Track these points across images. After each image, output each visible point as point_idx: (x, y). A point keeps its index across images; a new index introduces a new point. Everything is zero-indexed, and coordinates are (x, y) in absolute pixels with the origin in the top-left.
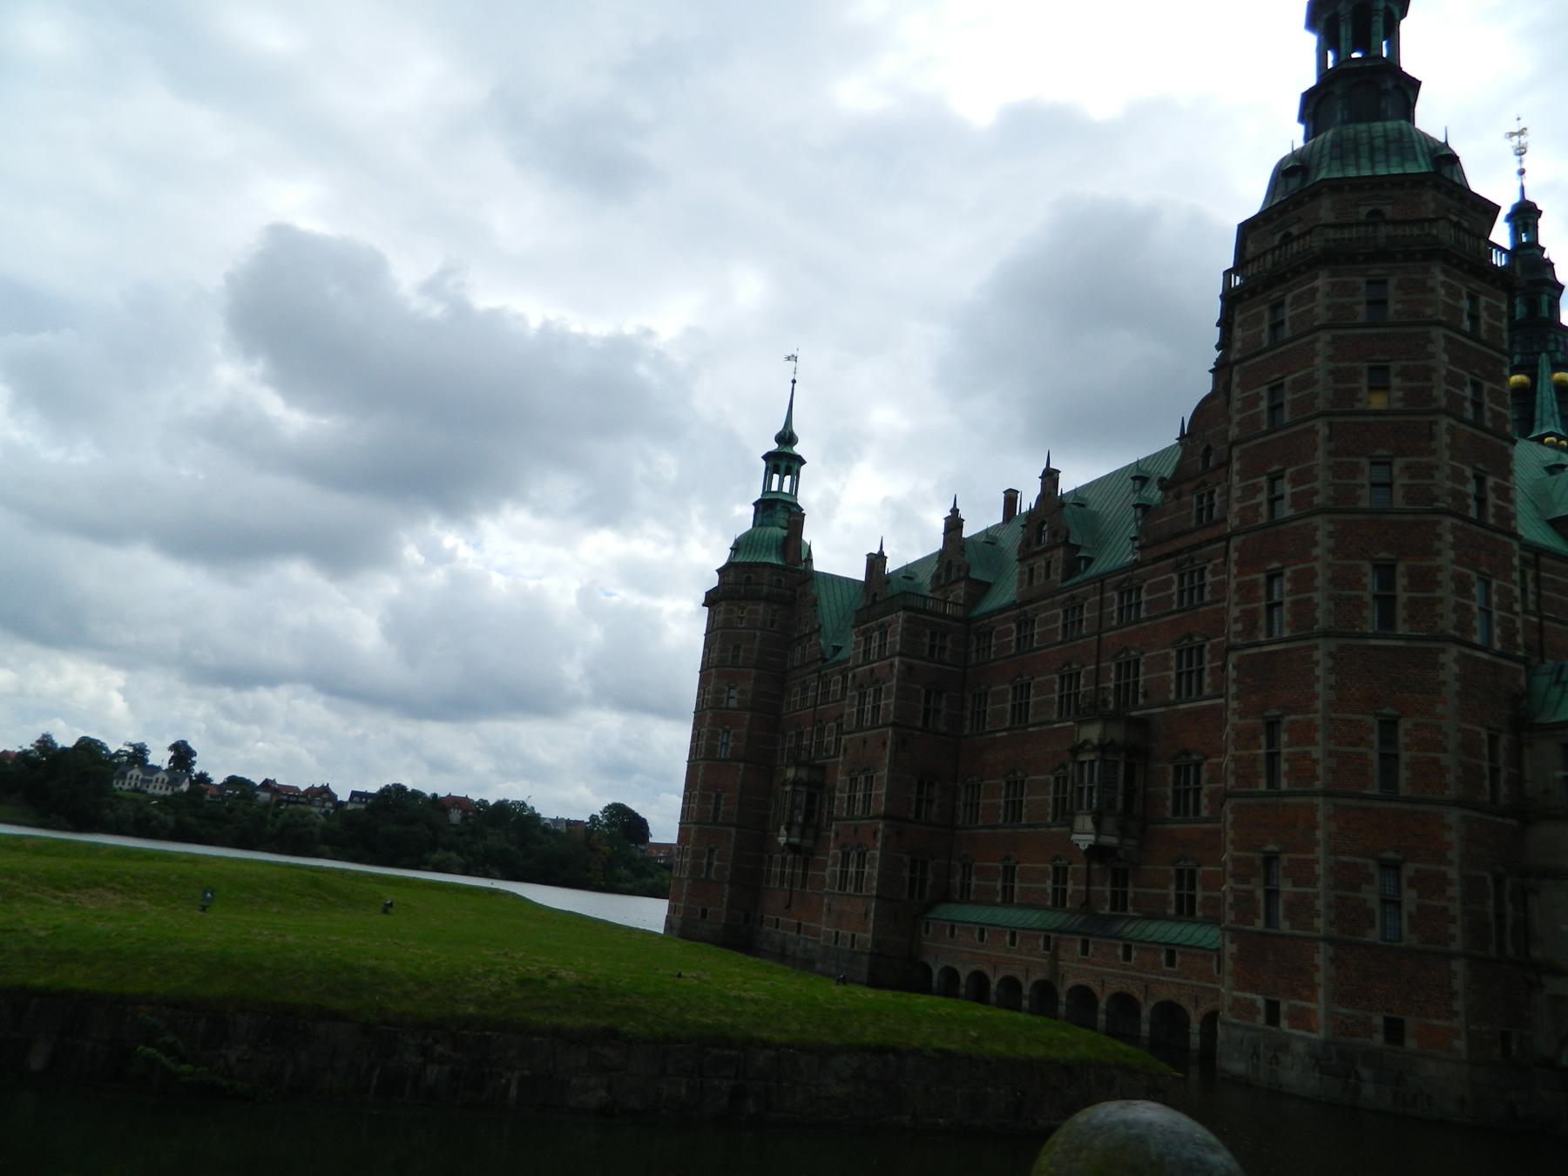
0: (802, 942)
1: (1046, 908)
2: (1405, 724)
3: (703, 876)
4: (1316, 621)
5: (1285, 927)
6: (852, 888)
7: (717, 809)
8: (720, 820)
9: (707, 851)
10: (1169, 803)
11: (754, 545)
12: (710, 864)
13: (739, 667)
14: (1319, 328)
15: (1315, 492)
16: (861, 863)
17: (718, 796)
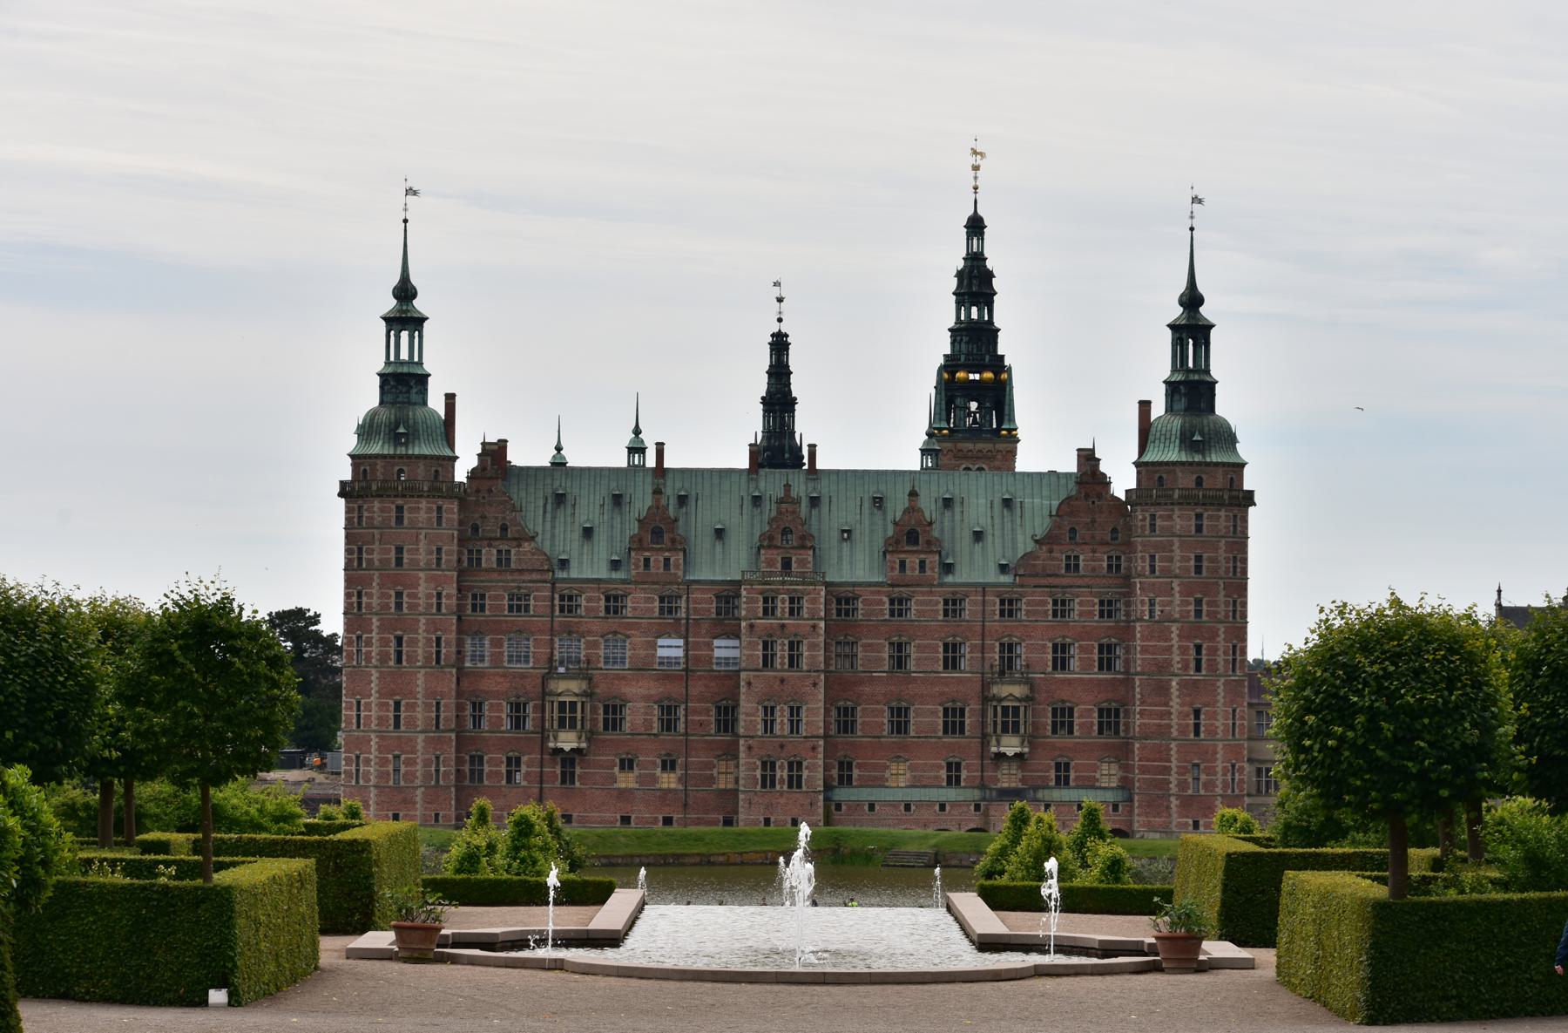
1: (942, 787)
2: (1238, 711)
3: (433, 783)
4: (1218, 670)
5: (1202, 792)
6: (785, 787)
7: (438, 717)
8: (441, 727)
9: (434, 759)
10: (1049, 728)
11: (429, 431)
12: (437, 771)
13: (443, 570)
14: (1223, 537)
15: (1219, 613)
17: (438, 704)
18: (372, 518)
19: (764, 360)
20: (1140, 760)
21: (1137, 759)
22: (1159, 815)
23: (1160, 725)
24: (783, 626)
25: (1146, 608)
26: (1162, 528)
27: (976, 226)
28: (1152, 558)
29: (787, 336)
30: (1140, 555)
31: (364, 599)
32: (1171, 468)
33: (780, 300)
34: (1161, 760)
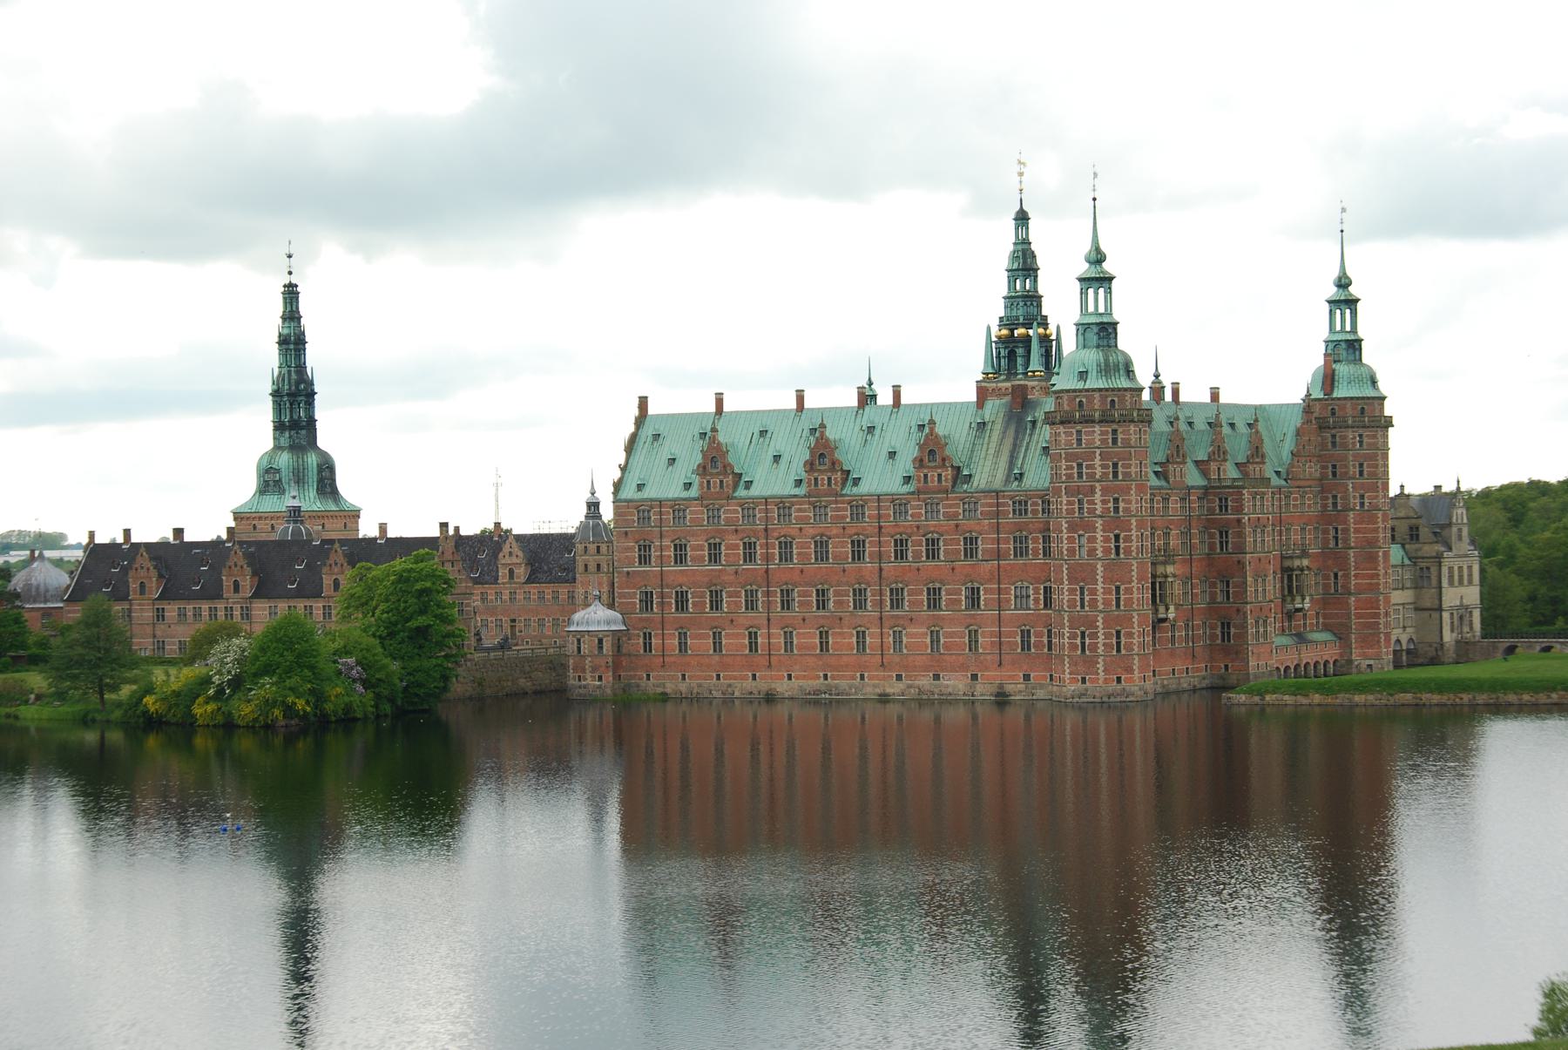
0: (1159, 682)
16: (1265, 625)
18: (1130, 440)
19: (278, 307)
20: (1356, 609)
21: (1353, 608)
22: (1371, 647)
23: (1371, 584)
24: (1259, 518)
25: (1358, 501)
26: (1369, 444)
27: (1022, 218)
28: (1361, 465)
29: (296, 286)
30: (1351, 463)
31: (1122, 505)
32: (1371, 401)
33: (290, 256)
34: (1372, 608)
